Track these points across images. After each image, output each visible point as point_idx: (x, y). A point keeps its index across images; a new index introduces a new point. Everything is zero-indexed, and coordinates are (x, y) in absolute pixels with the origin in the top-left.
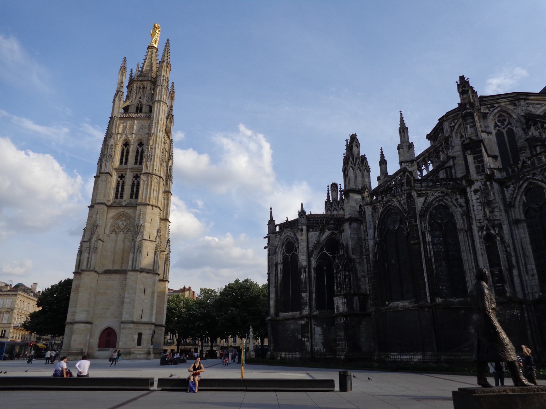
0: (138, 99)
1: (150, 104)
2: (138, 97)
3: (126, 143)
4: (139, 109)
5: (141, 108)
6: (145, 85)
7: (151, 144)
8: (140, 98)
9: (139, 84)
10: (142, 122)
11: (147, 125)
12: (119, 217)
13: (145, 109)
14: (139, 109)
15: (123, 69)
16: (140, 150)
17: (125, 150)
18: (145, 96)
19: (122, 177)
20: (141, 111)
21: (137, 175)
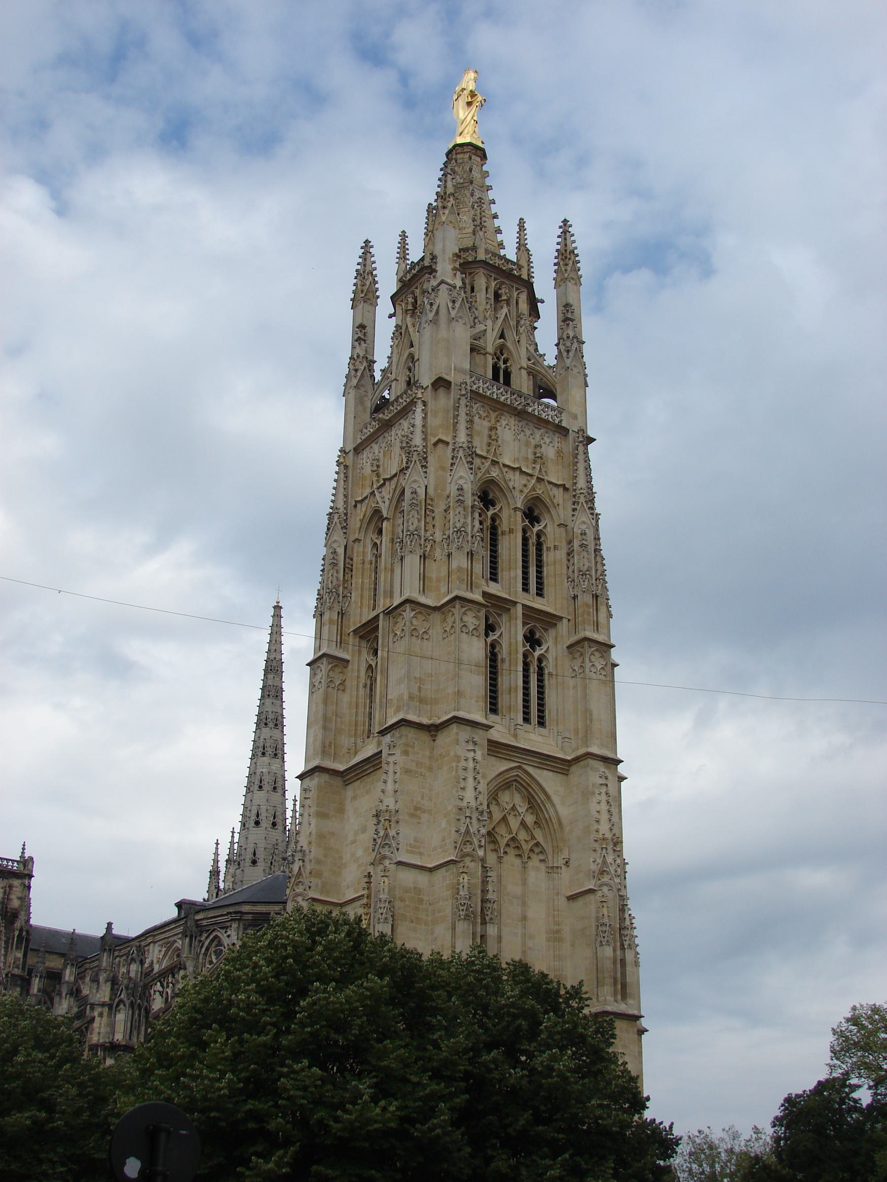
5: (507, 375)
8: (502, 336)
12: (505, 784)
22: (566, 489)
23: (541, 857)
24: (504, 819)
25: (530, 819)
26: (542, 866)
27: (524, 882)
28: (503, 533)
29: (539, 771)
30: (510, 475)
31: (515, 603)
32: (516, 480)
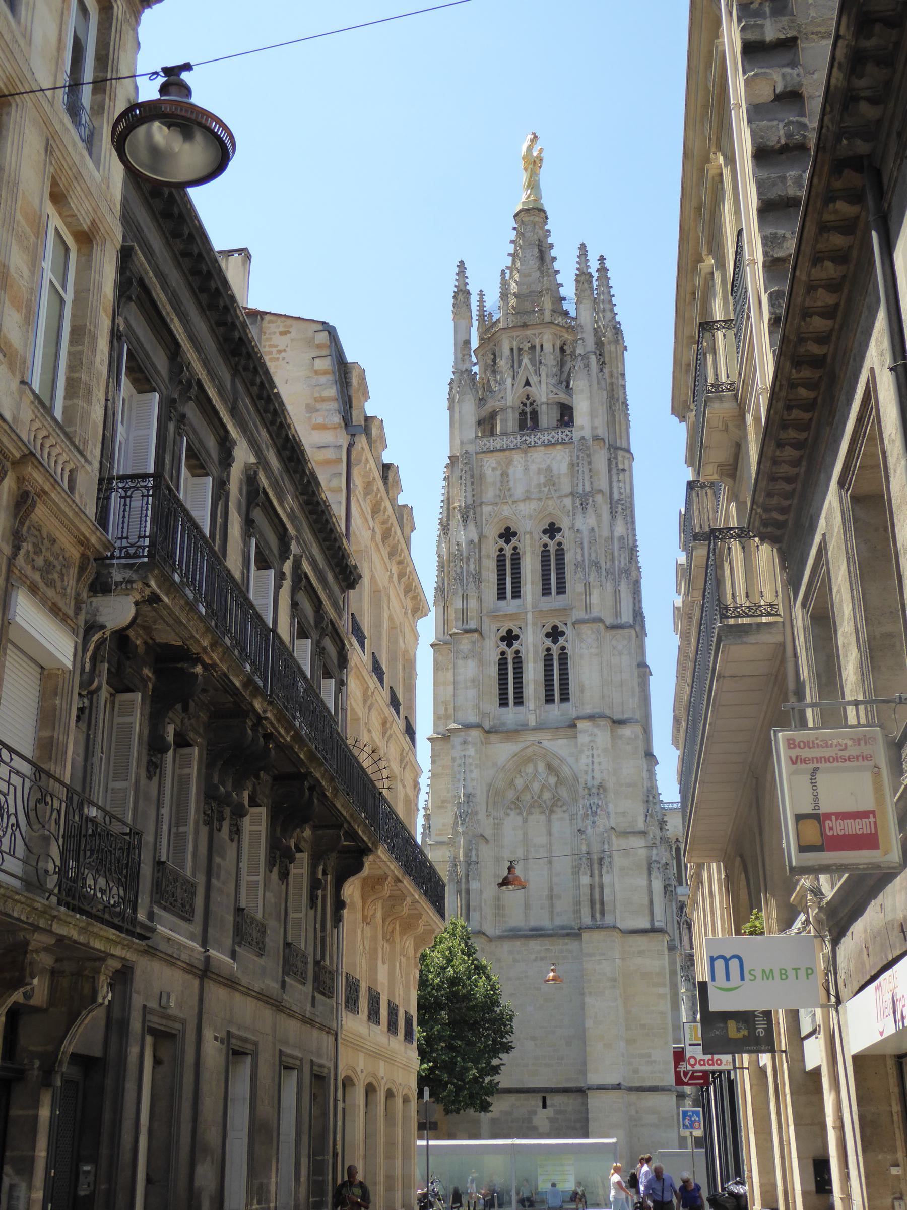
0: (521, 390)
1: (563, 397)
4: (528, 419)
5: (535, 415)
8: (527, 383)
13: (548, 417)
14: (528, 419)
15: (462, 295)
18: (543, 374)
20: (535, 426)
21: (555, 628)
23: (565, 808)
24: (527, 787)
25: (552, 780)
26: (567, 816)
27: (550, 834)
29: (552, 742)
30: (521, 506)
32: (525, 509)
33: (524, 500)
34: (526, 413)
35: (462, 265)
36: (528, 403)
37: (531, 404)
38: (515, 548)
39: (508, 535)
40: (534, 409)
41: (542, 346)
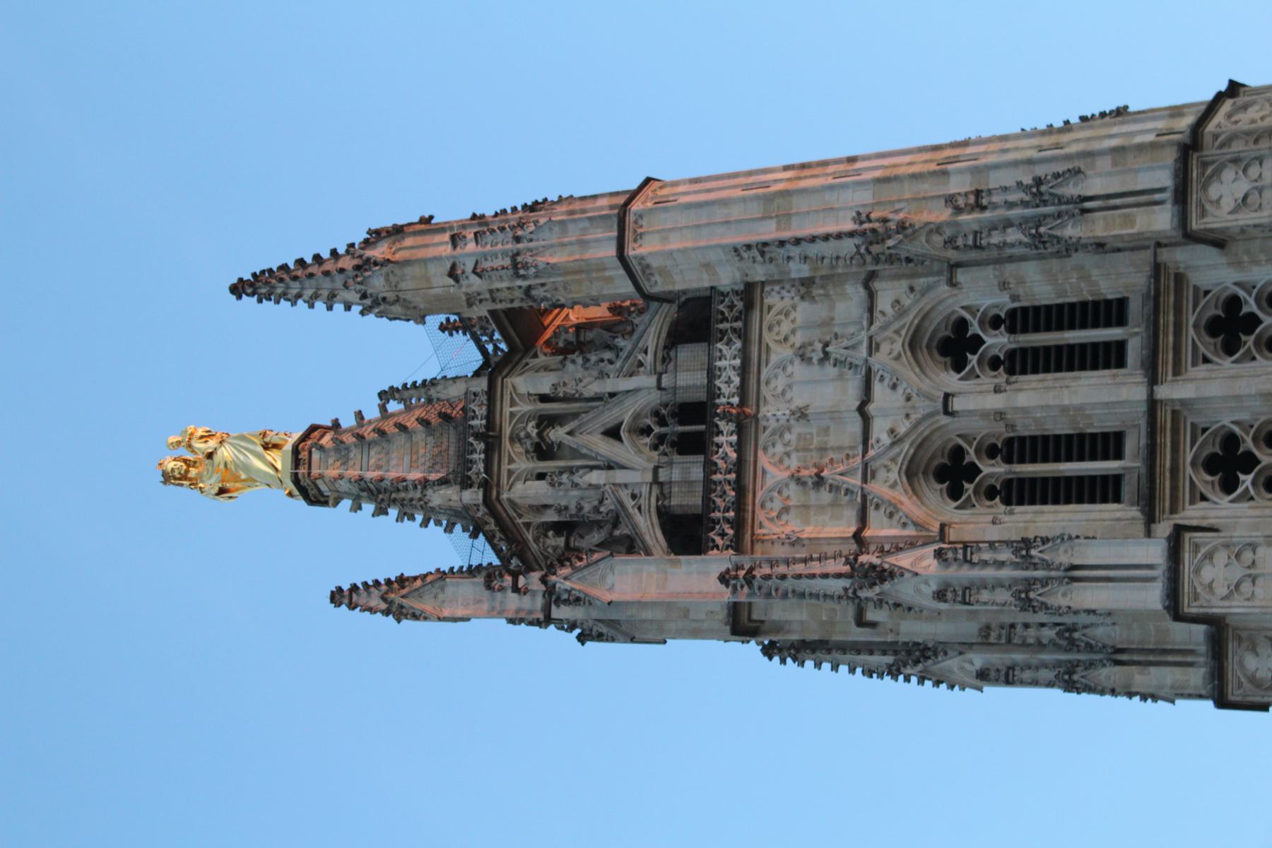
1: (653, 330)
2: (606, 448)
3: (941, 474)
6: (525, 408)
7: (942, 214)
8: (613, 433)
9: (517, 460)
10: (779, 353)
11: (804, 311)
16: (998, 342)
17: (994, 470)
18: (595, 388)
19: (1228, 463)
21: (1214, 327)
22: (872, 276)
28: (1012, 427)
31: (1153, 405)
33: (866, 420)
34: (683, 435)
35: (337, 597)
36: (657, 429)
37: (662, 422)
38: (992, 452)
39: (954, 473)
40: (673, 415)
41: (544, 398)
